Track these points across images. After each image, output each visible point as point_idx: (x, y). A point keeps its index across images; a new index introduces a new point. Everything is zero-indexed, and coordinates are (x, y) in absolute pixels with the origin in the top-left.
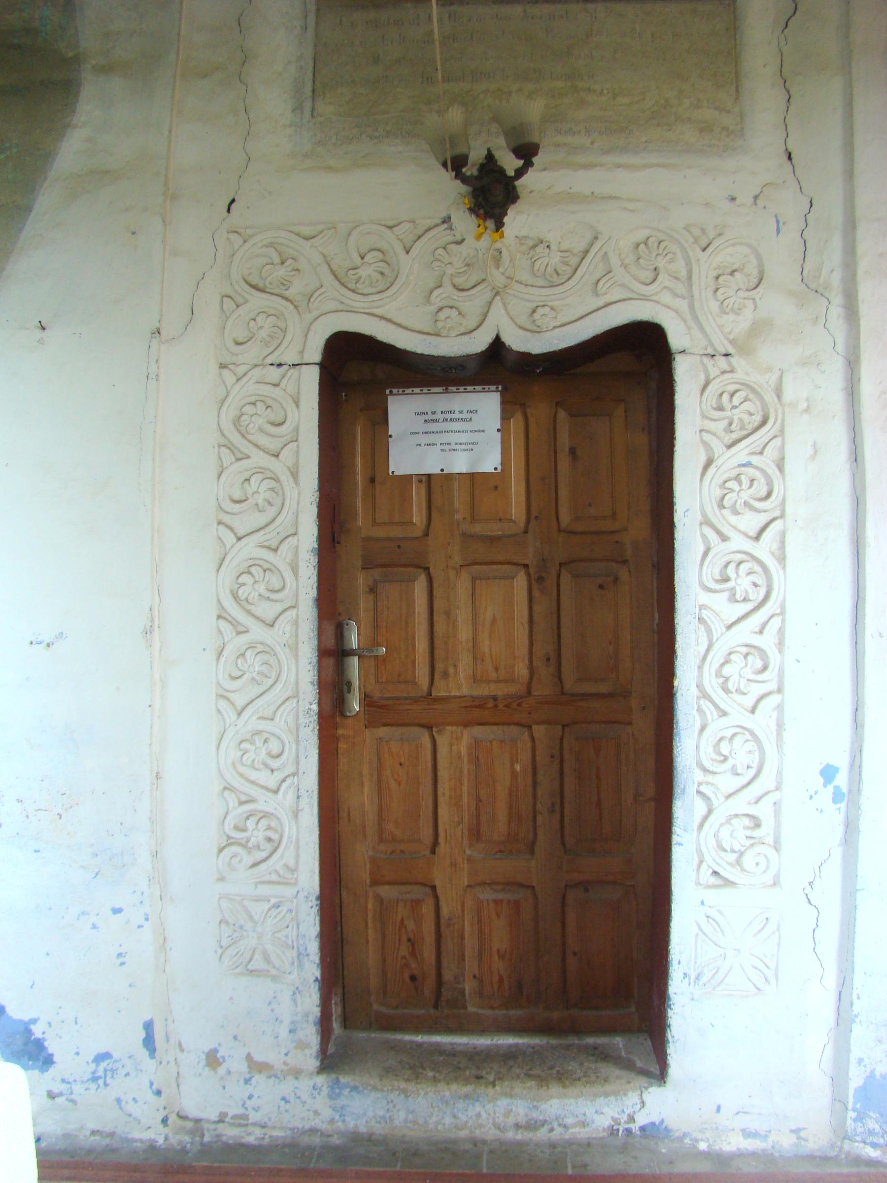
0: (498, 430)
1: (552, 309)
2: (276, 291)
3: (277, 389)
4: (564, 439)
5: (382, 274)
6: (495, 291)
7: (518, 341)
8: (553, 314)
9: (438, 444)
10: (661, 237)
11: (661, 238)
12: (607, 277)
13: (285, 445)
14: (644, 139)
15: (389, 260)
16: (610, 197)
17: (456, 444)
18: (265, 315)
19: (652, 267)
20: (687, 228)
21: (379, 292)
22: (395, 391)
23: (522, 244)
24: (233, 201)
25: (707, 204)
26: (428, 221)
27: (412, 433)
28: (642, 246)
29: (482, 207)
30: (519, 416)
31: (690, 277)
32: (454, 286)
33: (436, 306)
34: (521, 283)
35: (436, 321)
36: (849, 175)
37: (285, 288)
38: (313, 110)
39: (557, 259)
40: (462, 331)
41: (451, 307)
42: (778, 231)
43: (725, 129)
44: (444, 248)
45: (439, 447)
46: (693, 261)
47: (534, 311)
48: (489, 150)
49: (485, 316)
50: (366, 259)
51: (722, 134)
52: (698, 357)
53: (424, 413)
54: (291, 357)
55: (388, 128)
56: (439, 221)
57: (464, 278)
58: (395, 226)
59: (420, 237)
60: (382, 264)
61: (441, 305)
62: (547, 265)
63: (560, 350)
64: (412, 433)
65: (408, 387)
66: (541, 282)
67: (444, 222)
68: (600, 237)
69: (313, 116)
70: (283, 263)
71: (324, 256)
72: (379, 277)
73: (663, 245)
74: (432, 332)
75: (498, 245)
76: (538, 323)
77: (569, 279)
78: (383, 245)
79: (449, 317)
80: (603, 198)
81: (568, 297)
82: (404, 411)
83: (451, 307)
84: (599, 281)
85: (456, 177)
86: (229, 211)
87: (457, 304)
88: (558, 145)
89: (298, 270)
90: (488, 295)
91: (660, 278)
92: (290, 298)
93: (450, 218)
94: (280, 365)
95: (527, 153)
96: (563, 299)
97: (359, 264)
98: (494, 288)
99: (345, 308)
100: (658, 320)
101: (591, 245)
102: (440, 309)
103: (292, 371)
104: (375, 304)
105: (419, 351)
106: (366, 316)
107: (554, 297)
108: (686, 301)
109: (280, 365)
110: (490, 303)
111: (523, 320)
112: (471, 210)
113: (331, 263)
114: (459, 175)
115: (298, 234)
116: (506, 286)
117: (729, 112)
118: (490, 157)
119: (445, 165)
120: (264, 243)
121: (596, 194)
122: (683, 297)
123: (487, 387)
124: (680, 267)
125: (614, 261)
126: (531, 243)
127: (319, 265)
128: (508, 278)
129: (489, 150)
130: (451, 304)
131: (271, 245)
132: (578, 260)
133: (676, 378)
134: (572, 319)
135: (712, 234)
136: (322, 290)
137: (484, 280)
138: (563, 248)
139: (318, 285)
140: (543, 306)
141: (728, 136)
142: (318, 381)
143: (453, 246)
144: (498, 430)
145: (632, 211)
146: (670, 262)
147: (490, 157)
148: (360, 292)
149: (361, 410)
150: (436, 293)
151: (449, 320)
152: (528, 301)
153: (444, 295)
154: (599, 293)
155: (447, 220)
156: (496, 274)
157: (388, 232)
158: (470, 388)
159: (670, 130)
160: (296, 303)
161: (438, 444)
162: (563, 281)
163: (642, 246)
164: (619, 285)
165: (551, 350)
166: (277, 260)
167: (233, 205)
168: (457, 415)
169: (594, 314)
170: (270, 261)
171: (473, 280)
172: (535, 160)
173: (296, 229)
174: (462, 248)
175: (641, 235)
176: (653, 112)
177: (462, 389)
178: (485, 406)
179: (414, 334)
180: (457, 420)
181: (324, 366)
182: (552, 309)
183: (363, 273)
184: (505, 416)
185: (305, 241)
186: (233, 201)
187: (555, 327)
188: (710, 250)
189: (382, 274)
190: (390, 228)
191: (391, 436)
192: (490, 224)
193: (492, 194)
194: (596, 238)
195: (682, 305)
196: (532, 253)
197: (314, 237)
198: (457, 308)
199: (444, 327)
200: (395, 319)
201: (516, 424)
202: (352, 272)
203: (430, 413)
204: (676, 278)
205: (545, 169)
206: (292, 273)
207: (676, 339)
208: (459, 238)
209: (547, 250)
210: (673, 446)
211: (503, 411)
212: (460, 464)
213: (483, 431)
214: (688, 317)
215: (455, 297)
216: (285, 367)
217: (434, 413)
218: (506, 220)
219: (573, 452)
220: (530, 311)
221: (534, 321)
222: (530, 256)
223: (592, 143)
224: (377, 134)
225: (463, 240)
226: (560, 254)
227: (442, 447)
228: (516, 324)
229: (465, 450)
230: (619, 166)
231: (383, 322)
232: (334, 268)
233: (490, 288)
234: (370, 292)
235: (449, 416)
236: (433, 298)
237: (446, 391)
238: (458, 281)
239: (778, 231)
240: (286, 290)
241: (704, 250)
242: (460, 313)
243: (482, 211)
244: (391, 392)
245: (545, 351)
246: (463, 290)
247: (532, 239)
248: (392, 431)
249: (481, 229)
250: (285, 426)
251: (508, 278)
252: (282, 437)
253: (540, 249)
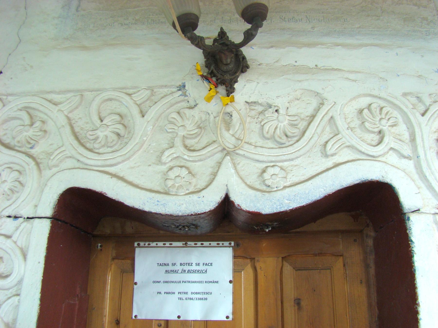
0: (230, 282)
1: (282, 168)
2: (23, 149)
3: (9, 241)
4: (290, 293)
5: (118, 135)
6: (225, 152)
7: (248, 201)
8: (282, 174)
9: (177, 293)
10: (382, 104)
11: (382, 106)
12: (335, 139)
13: (9, 298)
14: (357, 26)
15: (126, 123)
16: (333, 69)
17: (192, 293)
18: (9, 170)
19: (377, 130)
21: (113, 152)
22: (142, 244)
23: (253, 110)
26: (166, 90)
27: (154, 282)
28: (366, 111)
29: (215, 76)
30: (249, 270)
31: (413, 139)
32: (186, 147)
33: (168, 165)
34: (250, 144)
35: (167, 179)
37: (30, 146)
38: (79, 6)
39: (286, 122)
40: (190, 191)
41: (181, 167)
43: (425, 19)
44: (178, 113)
45: (177, 295)
46: (415, 125)
47: (264, 171)
48: (222, 29)
49: (214, 175)
50: (104, 122)
52: (432, 216)
53: (165, 264)
54: (26, 212)
55: (137, 18)
57: (196, 140)
58: (135, 93)
60: (120, 127)
61: (171, 164)
62: (276, 128)
63: (292, 211)
64: (154, 282)
65: (153, 241)
66: (270, 144)
68: (326, 103)
69: (77, 11)
71: (69, 119)
72: (115, 137)
73: (384, 111)
74: (162, 191)
75: (229, 109)
76: (267, 182)
77: (297, 141)
78: (123, 110)
79: (178, 176)
80: (326, 69)
81: (297, 158)
82: (148, 261)
83: (181, 167)
84: (327, 142)
87: (189, 164)
88: (284, 29)
89: (45, 131)
90: (219, 156)
91: (386, 140)
92: (35, 156)
93: (184, 86)
94: (16, 217)
96: (292, 160)
97: (98, 126)
98: (224, 149)
99: (81, 166)
100: (388, 180)
101: (317, 110)
102: (171, 169)
103: (25, 224)
104: (109, 162)
105: (147, 209)
106: (98, 174)
107: (284, 158)
108: (411, 162)
109: (16, 217)
110: (219, 164)
111: (253, 180)
113: (74, 125)
115: (50, 101)
116: (236, 147)
117: (425, 7)
120: (20, 107)
121: (319, 67)
122: (409, 158)
123: (221, 243)
124: (402, 129)
125: (341, 124)
126: (260, 109)
127: (63, 126)
128: (238, 139)
129: (222, 29)
130: (182, 164)
131: (26, 109)
132: (305, 123)
133: (413, 239)
134: (302, 178)
135: (428, 101)
136: (62, 149)
137: (214, 141)
138: (289, 114)
139: (60, 144)
140: (273, 166)
141: (428, 24)
142: (47, 235)
143: (187, 111)
144: (230, 282)
145: (355, 81)
146: (392, 126)
148: (97, 151)
149: (113, 259)
150: (167, 153)
151: (178, 179)
152: (258, 161)
153: (175, 155)
154: (328, 153)
156: (226, 135)
157: (127, 98)
158: (206, 243)
159: (379, 19)
160: (39, 161)
161: (177, 293)
162: (291, 143)
163: (366, 111)
164: (348, 147)
165: (282, 210)
166: (27, 121)
168: (194, 267)
169: (324, 174)
170: (22, 123)
171: (205, 141)
173: (49, 97)
174: (195, 112)
175: (364, 102)
176: (362, 7)
177: (199, 244)
178: (219, 260)
179: (143, 191)
180: (194, 272)
181: (57, 220)
182: (282, 168)
183: (101, 134)
184: (237, 270)
185: (54, 106)
187: (285, 187)
188: (428, 114)
189: (118, 135)
191: (136, 284)
192: (222, 89)
193: (223, 65)
194: (322, 104)
195: (410, 165)
196: (261, 117)
198: (187, 168)
199: (173, 186)
200: (126, 178)
201: (247, 274)
202: (91, 133)
203: (170, 265)
204: (400, 140)
205: (272, 47)
206: (39, 134)
207: (408, 198)
208: (192, 103)
209: (276, 114)
210: (417, 313)
211: (235, 264)
212: (195, 312)
213: (217, 282)
214: (416, 177)
215: (186, 157)
216: (21, 220)
217: (174, 264)
218: (236, 86)
219: (298, 302)
220: (260, 171)
221: (264, 181)
222: (260, 120)
223: (313, 28)
224: (127, 22)
226: (288, 118)
227: (180, 296)
228: (246, 183)
229: (200, 299)
230: (338, 45)
231: (114, 179)
232: (77, 129)
233: (220, 149)
234: (105, 151)
235: (187, 268)
236: (164, 159)
237: (186, 245)
238: (189, 142)
240: (31, 148)
241: (423, 115)
242: (190, 173)
244: (139, 244)
245: (275, 211)
246: (194, 151)
247: (261, 104)
248: (138, 278)
249: (212, 93)
250: (9, 280)
251: (238, 139)
252: (8, 289)
253: (270, 113)
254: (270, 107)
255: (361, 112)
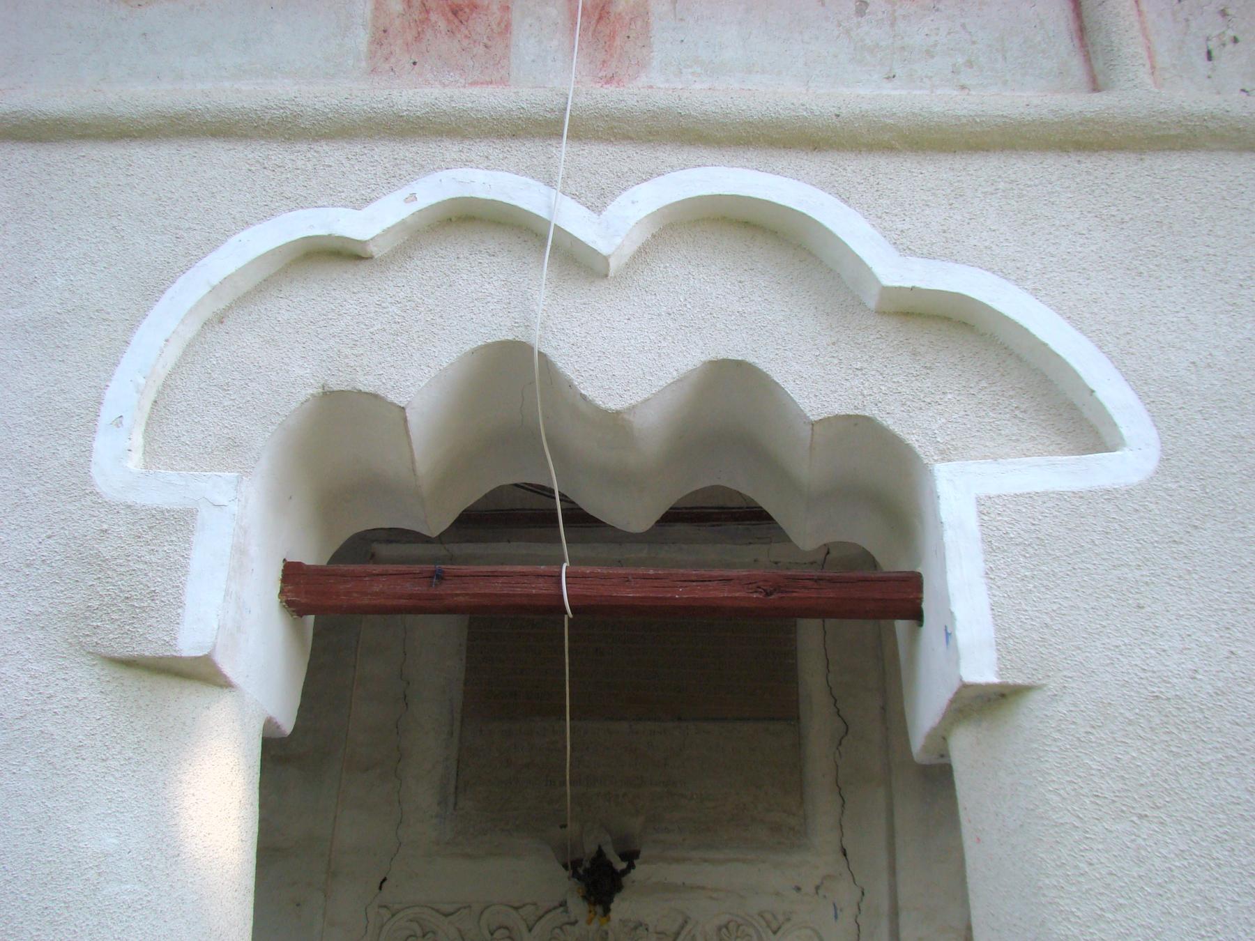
20: (761, 915)
24: (385, 880)
25: (777, 894)
28: (724, 930)
36: (893, 871)
38: (456, 804)
42: (836, 917)
48: (600, 847)
51: (788, 834)
56: (556, 904)
59: (541, 918)
67: (561, 905)
69: (455, 809)
70: (424, 936)
71: (459, 930)
85: (573, 876)
86: (380, 888)
95: (630, 857)
101: (682, 927)
112: (584, 897)
114: (575, 874)
115: (437, 911)
118: (600, 853)
119: (565, 866)
126: (632, 925)
129: (600, 847)
135: (781, 918)
147: (600, 853)
155: (563, 904)
157: (514, 912)
166: (419, 933)
167: (385, 884)
172: (636, 862)
175: (724, 919)
186: (385, 880)
188: (779, 933)
190: (516, 909)
192: (599, 909)
193: (600, 882)
197: (451, 914)
208: (572, 919)
218: (613, 906)
225: (576, 922)
230: (705, 861)
239: (836, 917)
241: (775, 933)
243: (592, 899)
254: (641, 925)
255: (720, 929)
